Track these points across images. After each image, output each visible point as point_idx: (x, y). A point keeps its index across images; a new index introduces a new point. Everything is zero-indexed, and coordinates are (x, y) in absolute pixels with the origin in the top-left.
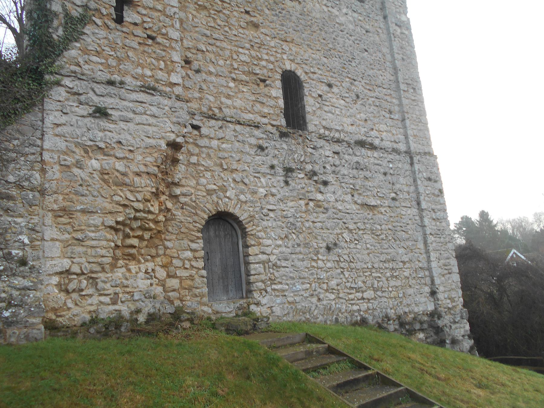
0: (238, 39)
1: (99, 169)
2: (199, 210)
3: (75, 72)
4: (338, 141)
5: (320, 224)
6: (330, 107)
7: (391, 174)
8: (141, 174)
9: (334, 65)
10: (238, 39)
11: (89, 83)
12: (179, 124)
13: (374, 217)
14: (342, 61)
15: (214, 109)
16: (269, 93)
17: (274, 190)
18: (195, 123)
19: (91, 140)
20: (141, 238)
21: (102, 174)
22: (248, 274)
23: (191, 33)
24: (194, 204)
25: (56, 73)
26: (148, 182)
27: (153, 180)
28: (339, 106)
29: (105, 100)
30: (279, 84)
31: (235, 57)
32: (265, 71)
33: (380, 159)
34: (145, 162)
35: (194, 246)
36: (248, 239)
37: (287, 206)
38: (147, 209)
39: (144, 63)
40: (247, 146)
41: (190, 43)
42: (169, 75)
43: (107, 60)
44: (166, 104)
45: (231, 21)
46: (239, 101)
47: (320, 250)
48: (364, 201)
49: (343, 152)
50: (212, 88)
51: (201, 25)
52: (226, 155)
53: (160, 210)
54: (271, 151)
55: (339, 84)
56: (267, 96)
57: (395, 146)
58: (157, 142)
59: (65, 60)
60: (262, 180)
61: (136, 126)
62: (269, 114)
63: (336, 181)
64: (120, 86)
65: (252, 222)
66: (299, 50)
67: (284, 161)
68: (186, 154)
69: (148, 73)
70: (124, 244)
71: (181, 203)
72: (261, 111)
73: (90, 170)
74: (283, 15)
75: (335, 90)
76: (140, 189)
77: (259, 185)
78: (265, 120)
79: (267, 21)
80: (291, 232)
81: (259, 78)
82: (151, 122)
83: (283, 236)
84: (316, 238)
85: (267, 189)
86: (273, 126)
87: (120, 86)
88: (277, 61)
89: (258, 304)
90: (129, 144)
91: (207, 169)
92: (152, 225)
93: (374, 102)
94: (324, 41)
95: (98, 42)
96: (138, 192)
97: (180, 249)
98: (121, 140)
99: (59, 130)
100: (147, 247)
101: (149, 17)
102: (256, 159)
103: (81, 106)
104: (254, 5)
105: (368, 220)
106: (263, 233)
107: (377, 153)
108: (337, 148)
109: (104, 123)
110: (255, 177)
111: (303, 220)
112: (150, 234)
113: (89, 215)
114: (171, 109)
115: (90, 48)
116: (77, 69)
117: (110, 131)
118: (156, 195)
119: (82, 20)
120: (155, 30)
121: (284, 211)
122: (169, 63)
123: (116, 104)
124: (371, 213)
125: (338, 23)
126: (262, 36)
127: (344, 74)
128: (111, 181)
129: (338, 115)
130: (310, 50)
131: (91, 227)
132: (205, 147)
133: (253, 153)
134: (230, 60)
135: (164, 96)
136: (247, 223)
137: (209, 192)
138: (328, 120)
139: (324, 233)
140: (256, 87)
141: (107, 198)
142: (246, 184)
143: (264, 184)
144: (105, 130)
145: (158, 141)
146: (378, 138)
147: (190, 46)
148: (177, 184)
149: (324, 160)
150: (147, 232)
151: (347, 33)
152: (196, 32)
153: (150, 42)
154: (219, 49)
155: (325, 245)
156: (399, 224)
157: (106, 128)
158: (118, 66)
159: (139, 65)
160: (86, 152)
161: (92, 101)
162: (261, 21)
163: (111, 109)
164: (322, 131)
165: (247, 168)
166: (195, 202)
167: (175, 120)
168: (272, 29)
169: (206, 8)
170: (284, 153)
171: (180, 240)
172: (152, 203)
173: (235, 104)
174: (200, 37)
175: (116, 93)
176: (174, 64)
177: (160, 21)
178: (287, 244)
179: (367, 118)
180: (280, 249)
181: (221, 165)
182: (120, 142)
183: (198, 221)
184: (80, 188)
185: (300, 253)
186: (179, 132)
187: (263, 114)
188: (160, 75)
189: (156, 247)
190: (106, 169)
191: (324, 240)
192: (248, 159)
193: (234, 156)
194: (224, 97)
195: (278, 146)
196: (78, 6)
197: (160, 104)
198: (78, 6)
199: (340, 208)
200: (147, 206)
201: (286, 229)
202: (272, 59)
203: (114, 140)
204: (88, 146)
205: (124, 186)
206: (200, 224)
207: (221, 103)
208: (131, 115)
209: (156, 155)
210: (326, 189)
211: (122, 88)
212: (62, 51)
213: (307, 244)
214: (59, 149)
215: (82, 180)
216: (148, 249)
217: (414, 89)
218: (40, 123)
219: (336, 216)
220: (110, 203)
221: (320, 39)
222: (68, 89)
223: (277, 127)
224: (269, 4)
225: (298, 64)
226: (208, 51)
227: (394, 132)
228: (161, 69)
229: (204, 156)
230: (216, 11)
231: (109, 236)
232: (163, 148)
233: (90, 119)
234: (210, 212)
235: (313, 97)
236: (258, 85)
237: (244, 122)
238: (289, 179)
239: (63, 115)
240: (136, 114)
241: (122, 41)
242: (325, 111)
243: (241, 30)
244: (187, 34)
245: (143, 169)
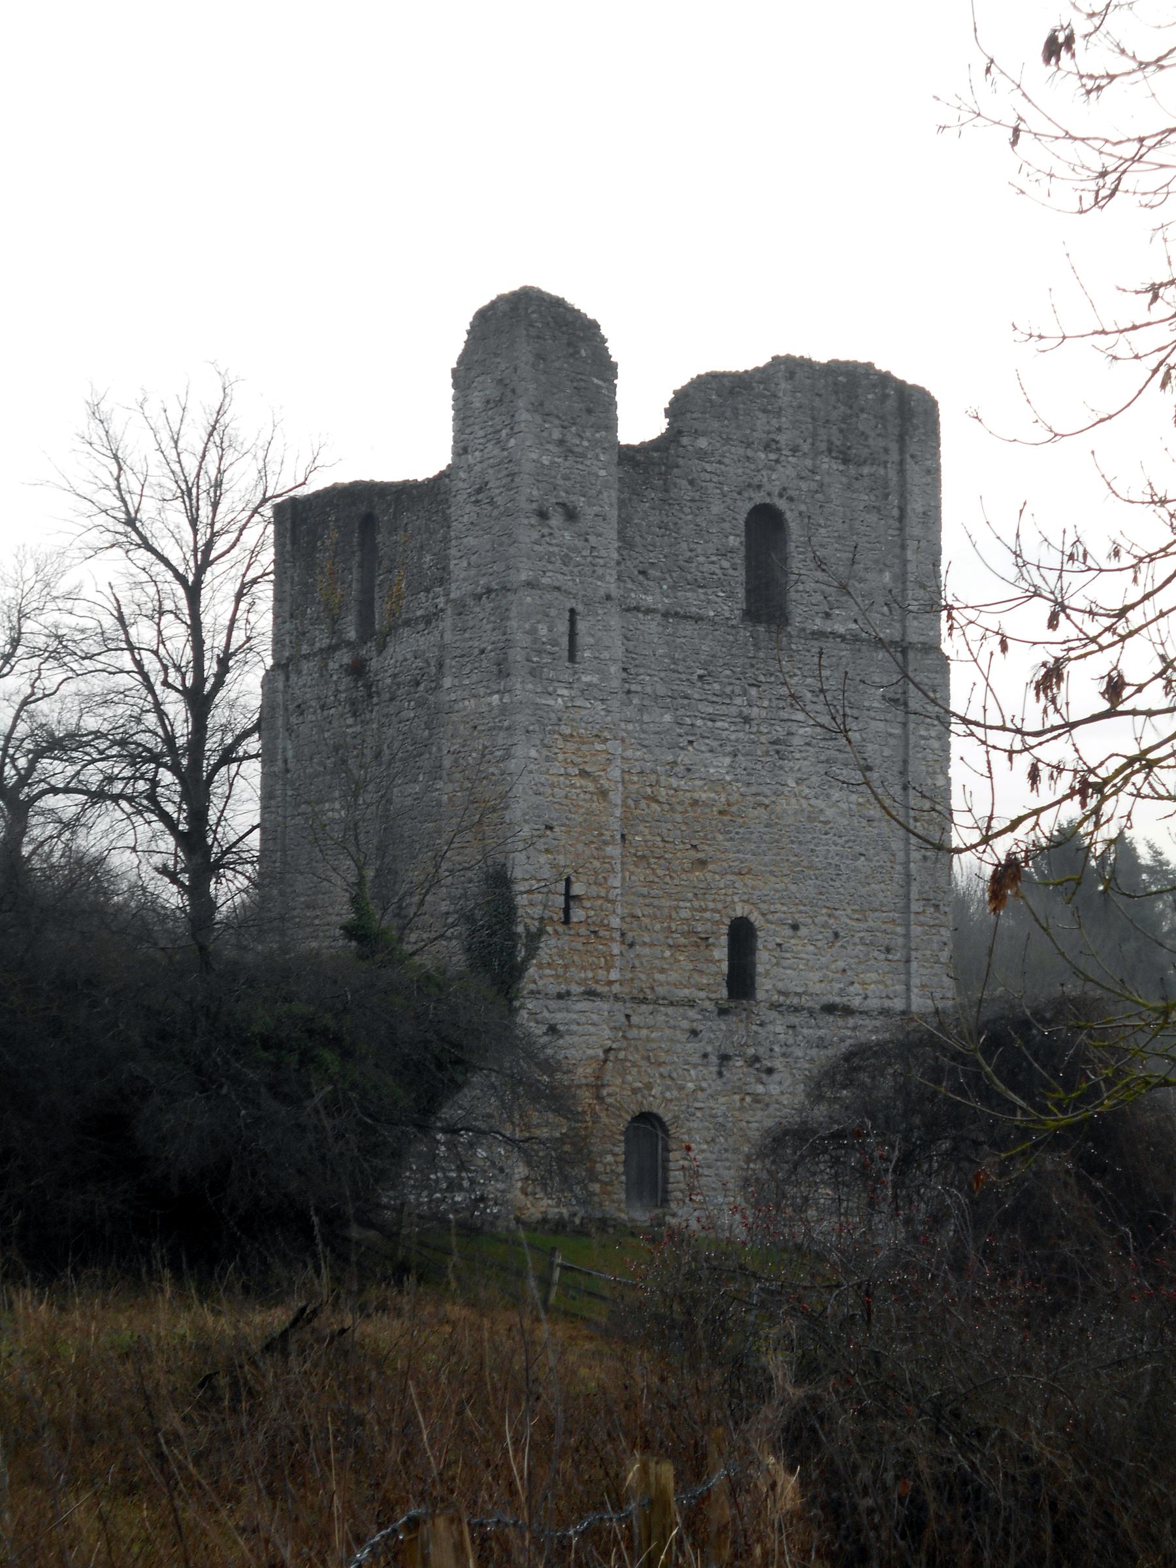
4: (797, 1010)
10: (679, 888)
14: (819, 883)
17: (704, 1085)
22: (666, 1181)
28: (805, 956)
30: (724, 940)
31: (674, 915)
42: (608, 972)
52: (654, 1046)
54: (705, 1035)
57: (887, 1003)
60: (692, 1072)
69: (590, 975)
75: (803, 931)
86: (711, 999)
89: (674, 1215)
108: (794, 1019)
126: (709, 876)
130: (773, 879)
137: (635, 1091)
165: (676, 1059)
167: (613, 1024)
174: (636, 899)
181: (648, 1058)
185: (727, 1160)
188: (601, 973)
202: (720, 906)
209: (594, 1065)
229: (631, 1049)
245: (584, 1081)
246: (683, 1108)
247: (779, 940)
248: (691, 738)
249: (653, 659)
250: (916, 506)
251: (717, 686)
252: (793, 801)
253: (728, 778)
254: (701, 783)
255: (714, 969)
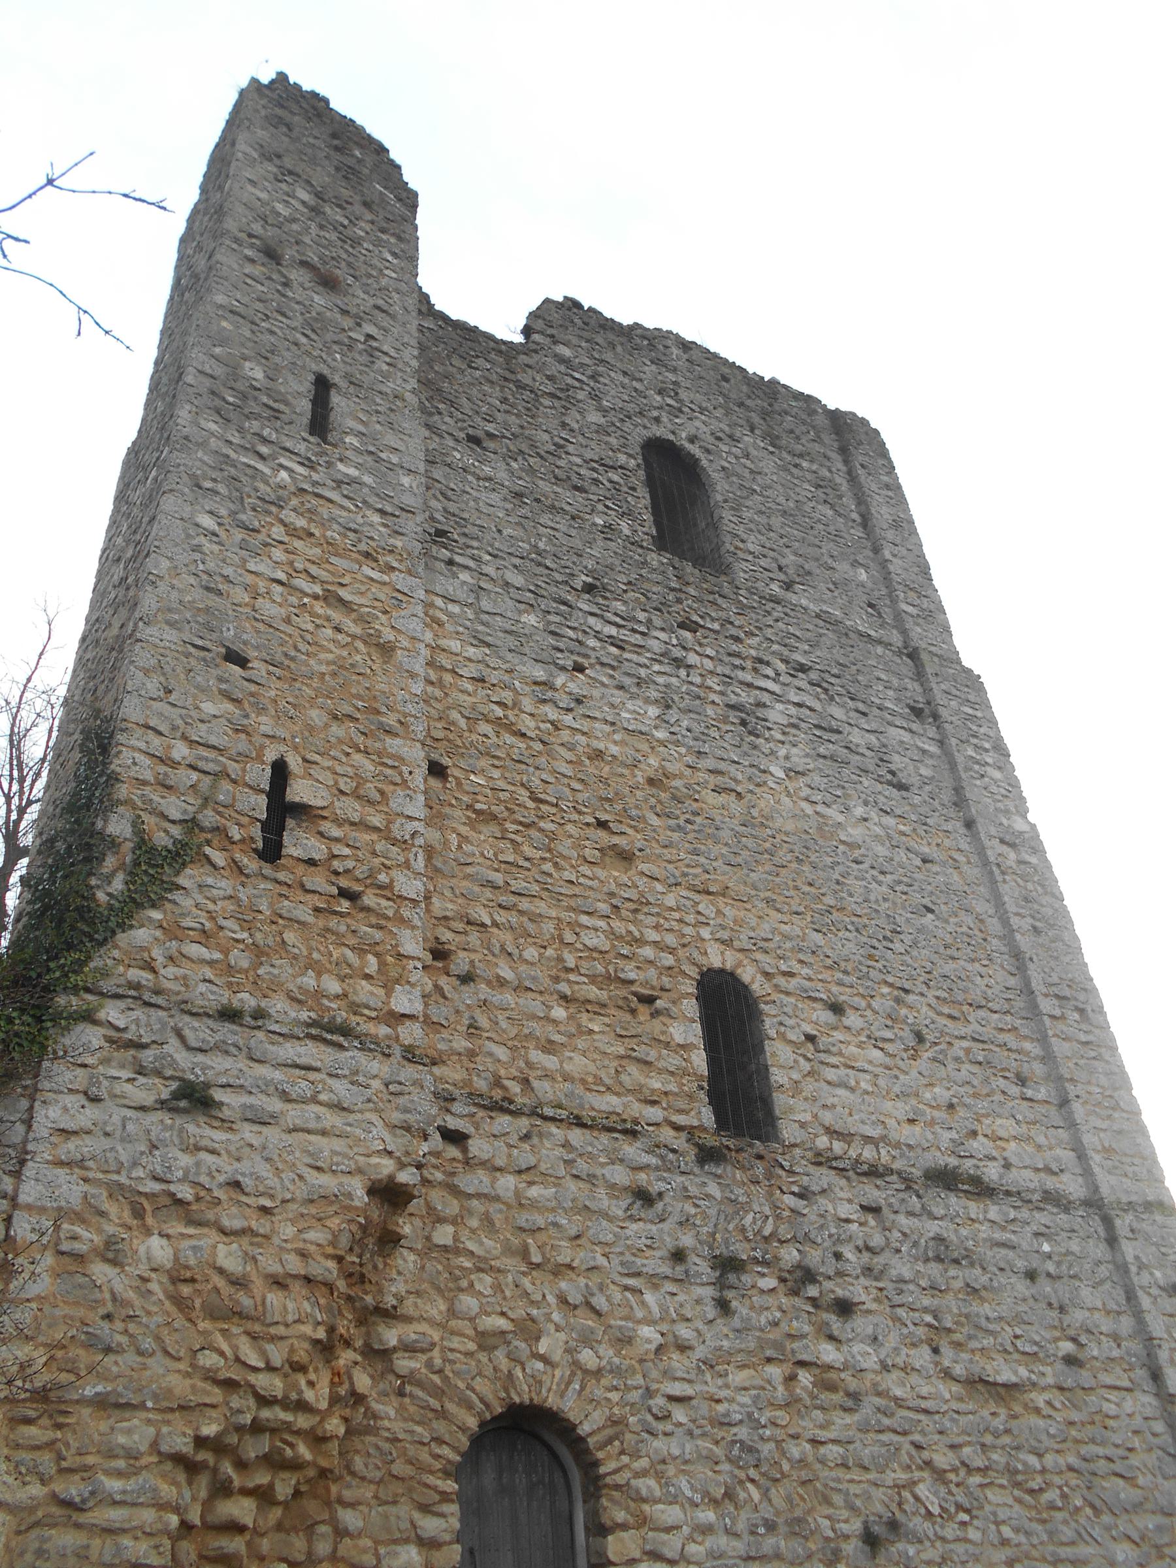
0: (577, 890)
1: (169, 1265)
2: (451, 1400)
3: (137, 986)
4: (874, 1172)
5: (837, 1449)
6: (843, 1071)
7: (1049, 1275)
8: (289, 1281)
9: (845, 952)
10: (577, 890)
11: (172, 1016)
12: (408, 1129)
13: (1013, 1424)
14: (865, 939)
15: (507, 1083)
16: (663, 1033)
17: (685, 1332)
18: (452, 1123)
19: (156, 1179)
20: (264, 1496)
21: (176, 1280)
23: (454, 881)
24: (436, 1379)
25: (87, 990)
26: (307, 1306)
27: (322, 1301)
28: (867, 1067)
29: (209, 1063)
30: (691, 1007)
31: (569, 937)
32: (652, 973)
33: (1011, 1227)
34: (301, 1245)
35: (430, 1526)
36: (604, 1501)
37: (727, 1386)
38: (294, 1396)
39: (324, 960)
40: (601, 1192)
41: (450, 906)
43: (226, 952)
44: (375, 1072)
45: (560, 848)
46: (578, 1059)
47: (844, 1546)
48: (976, 1370)
49: (890, 1205)
50: (504, 1024)
51: (481, 860)
52: (541, 1221)
53: (334, 1400)
54: (677, 1207)
55: (863, 1004)
56: (660, 1041)
57: (1051, 1183)
58: (341, 1184)
59: (116, 953)
60: (649, 1297)
61: (285, 1136)
62: (666, 1093)
63: (877, 1300)
64: (253, 1023)
65: (617, 1443)
66: (742, 913)
67: (713, 1235)
68: (422, 1217)
69: (333, 986)
70: (209, 1519)
71: (399, 1376)
72: (641, 1086)
73: (143, 1269)
74: (696, 827)
75: (852, 1019)
76: (281, 1330)
77: (639, 1314)
78: (654, 1113)
79: (654, 845)
80: (743, 1476)
81: (635, 994)
82: (327, 1124)
83: (719, 1492)
84: (827, 1501)
85: (664, 1328)
86: (677, 1128)
87: (253, 1023)
88: (684, 946)
90: (261, 1189)
91: (483, 1266)
92: (304, 1451)
93: (968, 1051)
94: (812, 890)
95: (211, 906)
96: (273, 1339)
97: (384, 1536)
98: (240, 1178)
99: (71, 1148)
100: (279, 1527)
101: (348, 846)
102: (628, 1232)
103: (142, 1080)
104: (618, 807)
105: (997, 1435)
106: (652, 1482)
107: (996, 1208)
108: (872, 1193)
109: (198, 1129)
110: (626, 1288)
111: (779, 1433)
112: (293, 1482)
113: (117, 1413)
114: (387, 1085)
115: (187, 922)
116: (145, 977)
117: (213, 1152)
118: (326, 1349)
119: (178, 854)
120: (361, 876)
121: (718, 1401)
122: (389, 959)
123: (236, 1072)
124: (1003, 1412)
125: (843, 842)
126: (641, 882)
127: (873, 974)
128: (198, 1303)
129: (868, 1093)
130: (773, 913)
131: (116, 1457)
132: (478, 1196)
133: (620, 1213)
134: (556, 946)
135: (371, 1050)
136: (602, 1446)
137: (487, 1341)
138: (839, 1109)
139: (852, 1481)
140: (628, 1017)
141: (179, 1359)
142: (598, 1313)
143: (656, 1310)
144: (198, 1148)
145: (345, 1179)
146: (994, 1159)
147: (448, 914)
148: (389, 1315)
149: (834, 1231)
150: (285, 1475)
151: (873, 868)
152: (467, 877)
153: (344, 905)
154: (525, 919)
155: (856, 1526)
156: (1101, 1451)
157: (204, 1143)
158: (255, 970)
159: (311, 965)
160: (138, 1213)
161: (173, 1063)
162: (639, 845)
163: (222, 1086)
164: (823, 1142)
165: (601, 1261)
166: (440, 1372)
167: (396, 1117)
168: (670, 862)
169: (494, 817)
170: (713, 1212)
171: (386, 1503)
172: (312, 1376)
173: (568, 1067)
174: (477, 889)
175: (241, 1043)
176: (405, 961)
177: (374, 853)
178: (733, 1523)
179: (955, 1100)
180: (709, 1542)
181: (524, 1253)
182: (237, 1185)
183: (447, 1438)
184: (106, 1325)
186: (407, 1153)
187: (648, 1093)
188: (365, 991)
189: (310, 1530)
190: (187, 1267)
191: (852, 1508)
192: (605, 1231)
193: (564, 1222)
194: (536, 1048)
195: (693, 1190)
196: (173, 822)
197: (357, 1073)
198: (173, 822)
199: (898, 1392)
200: (295, 1386)
201: (725, 1467)
202: (671, 940)
203: (221, 1178)
204: (146, 1195)
205: (236, 1320)
206: (454, 1448)
207: (529, 1064)
208: (276, 1105)
209: (334, 1223)
210: (848, 1326)
211: (259, 1027)
212: (114, 933)
213: (799, 1521)
214: (63, 1204)
215: (114, 1299)
216: (282, 1535)
217: (1082, 1011)
218: (20, 1128)
219: (886, 1421)
220: (187, 1375)
221: (799, 883)
222: (113, 1033)
223: (690, 1131)
224: (660, 802)
225: (742, 950)
226: (495, 924)
227: (1041, 1140)
228: (368, 977)
230: (521, 823)
231: (167, 1491)
232: (357, 1203)
233: (159, 1115)
234: (487, 1405)
235: (791, 1041)
236: (633, 1012)
237: (593, 1119)
238: (730, 1294)
239: (86, 1103)
240: (290, 1101)
241: (271, 905)
242: (829, 1083)
243: (585, 869)
244: (441, 882)
245: (294, 1264)
246: (635, 1396)
247: (809, 1029)
248: (580, 660)
249: (496, 535)
250: (882, 513)
251: (619, 606)
252: (786, 800)
253: (660, 734)
254: (608, 728)
255: (673, 1061)
